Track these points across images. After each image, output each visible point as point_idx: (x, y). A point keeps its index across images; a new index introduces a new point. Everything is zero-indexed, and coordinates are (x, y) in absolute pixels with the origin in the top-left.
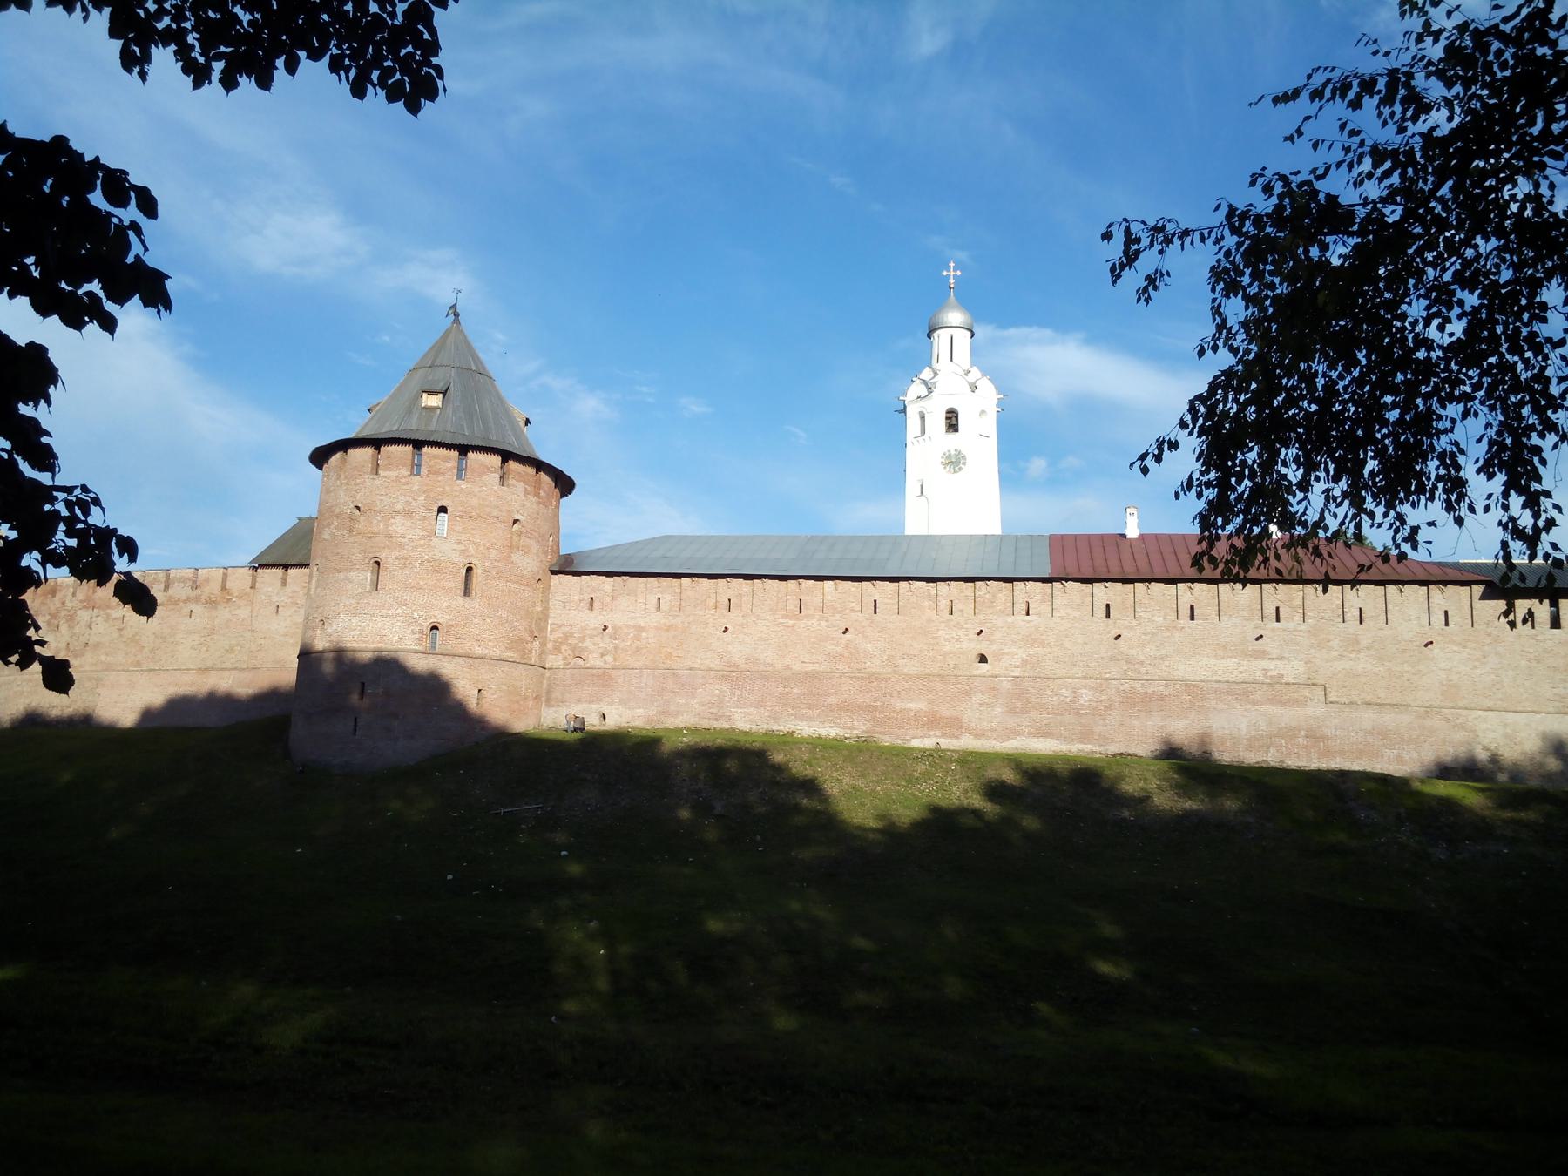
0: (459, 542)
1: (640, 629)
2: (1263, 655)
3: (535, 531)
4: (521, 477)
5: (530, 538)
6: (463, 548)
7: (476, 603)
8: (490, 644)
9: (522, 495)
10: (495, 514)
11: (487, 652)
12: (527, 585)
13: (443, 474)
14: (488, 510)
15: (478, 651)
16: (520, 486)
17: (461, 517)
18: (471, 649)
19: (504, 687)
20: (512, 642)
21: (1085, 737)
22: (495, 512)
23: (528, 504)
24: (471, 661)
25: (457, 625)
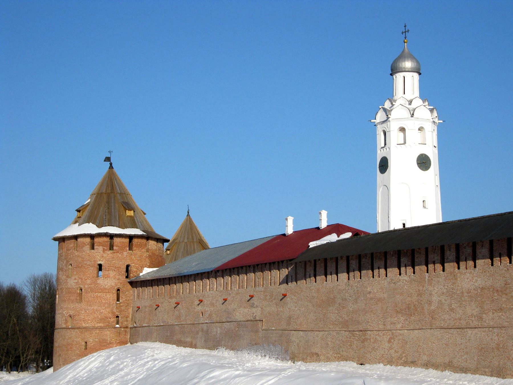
0: (75, 279)
1: (146, 307)
2: (252, 306)
3: (111, 266)
4: (100, 244)
5: (108, 271)
6: (77, 281)
8: (89, 322)
9: (102, 252)
11: (88, 325)
12: (108, 292)
13: (70, 250)
14: (85, 262)
15: (84, 325)
16: (101, 248)
17: (76, 268)
18: (81, 325)
19: (97, 340)
20: (100, 319)
22: (88, 263)
25: (76, 315)
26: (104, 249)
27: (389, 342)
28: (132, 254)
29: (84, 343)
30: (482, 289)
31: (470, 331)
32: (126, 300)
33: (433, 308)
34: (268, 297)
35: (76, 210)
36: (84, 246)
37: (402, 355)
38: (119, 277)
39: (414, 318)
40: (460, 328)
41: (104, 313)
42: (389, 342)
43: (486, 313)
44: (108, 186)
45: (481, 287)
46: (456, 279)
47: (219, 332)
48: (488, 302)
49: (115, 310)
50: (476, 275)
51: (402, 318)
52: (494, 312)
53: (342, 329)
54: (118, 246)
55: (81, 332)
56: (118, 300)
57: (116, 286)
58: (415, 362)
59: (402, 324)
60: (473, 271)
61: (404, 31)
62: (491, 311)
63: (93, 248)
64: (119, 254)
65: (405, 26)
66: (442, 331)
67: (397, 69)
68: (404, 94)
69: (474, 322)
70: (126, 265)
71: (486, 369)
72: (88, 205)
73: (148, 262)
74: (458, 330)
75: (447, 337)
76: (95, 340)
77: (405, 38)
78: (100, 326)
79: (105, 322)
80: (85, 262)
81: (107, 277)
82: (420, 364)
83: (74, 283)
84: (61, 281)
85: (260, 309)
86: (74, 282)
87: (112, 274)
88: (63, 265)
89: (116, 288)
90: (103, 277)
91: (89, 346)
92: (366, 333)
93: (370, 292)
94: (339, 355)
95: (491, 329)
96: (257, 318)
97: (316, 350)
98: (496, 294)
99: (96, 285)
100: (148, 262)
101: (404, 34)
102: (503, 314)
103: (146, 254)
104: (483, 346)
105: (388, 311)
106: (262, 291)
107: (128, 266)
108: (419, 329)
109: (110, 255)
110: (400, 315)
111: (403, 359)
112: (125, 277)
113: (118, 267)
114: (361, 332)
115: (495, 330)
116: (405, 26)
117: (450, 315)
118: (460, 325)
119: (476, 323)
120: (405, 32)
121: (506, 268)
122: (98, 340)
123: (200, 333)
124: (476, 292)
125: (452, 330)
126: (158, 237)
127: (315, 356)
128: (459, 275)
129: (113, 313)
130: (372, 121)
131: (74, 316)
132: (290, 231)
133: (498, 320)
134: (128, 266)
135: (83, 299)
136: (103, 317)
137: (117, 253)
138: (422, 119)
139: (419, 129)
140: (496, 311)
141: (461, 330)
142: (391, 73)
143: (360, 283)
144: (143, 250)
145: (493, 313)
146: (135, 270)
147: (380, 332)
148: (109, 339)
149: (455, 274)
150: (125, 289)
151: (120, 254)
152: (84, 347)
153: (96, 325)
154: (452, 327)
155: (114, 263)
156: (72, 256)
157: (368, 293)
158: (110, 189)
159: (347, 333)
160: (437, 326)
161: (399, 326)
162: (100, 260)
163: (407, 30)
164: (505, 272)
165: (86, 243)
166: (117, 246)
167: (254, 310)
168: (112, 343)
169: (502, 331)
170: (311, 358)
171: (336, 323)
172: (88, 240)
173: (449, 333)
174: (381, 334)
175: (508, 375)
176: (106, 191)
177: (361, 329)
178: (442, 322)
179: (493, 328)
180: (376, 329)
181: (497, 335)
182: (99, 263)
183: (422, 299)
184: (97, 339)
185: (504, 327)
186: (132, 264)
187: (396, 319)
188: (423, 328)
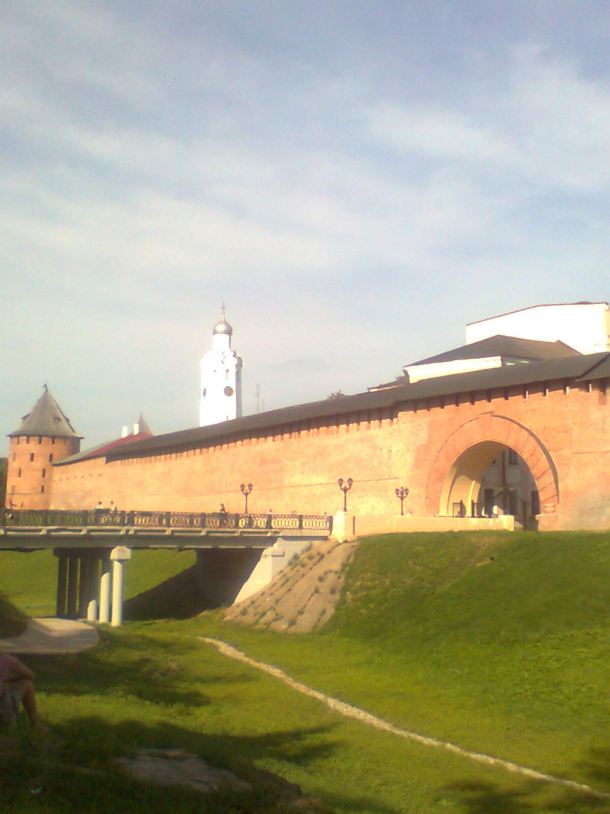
172: (25, 438)
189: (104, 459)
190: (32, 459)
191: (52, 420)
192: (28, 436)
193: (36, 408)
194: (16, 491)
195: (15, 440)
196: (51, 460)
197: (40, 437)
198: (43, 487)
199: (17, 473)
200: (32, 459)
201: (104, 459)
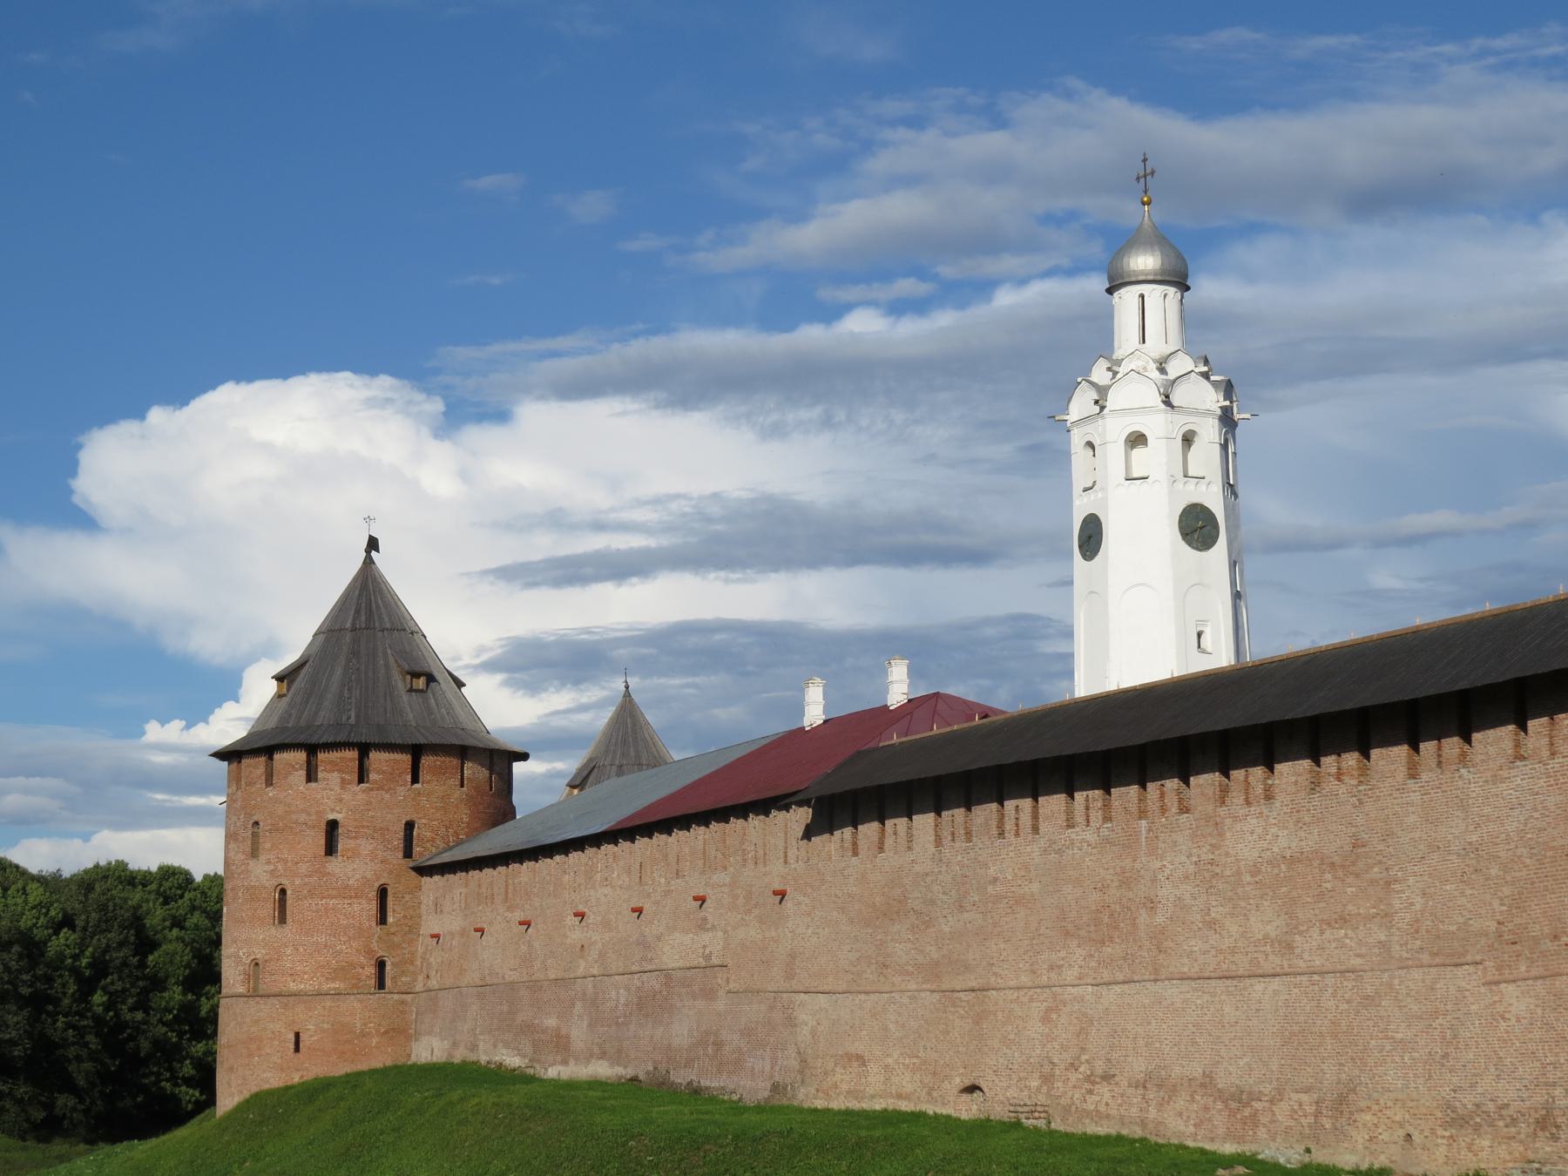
0: (268, 862)
1: (452, 934)
2: (702, 926)
3: (363, 827)
4: (334, 766)
5: (355, 838)
6: (272, 867)
7: (289, 931)
8: (306, 976)
9: (337, 788)
10: (303, 820)
11: (302, 987)
14: (294, 817)
15: (293, 986)
16: (335, 778)
18: (285, 986)
19: (325, 1026)
20: (335, 970)
21: (618, 1058)
22: (303, 818)
23: (346, 796)
24: (285, 1000)
26: (344, 783)
27: (1046, 1019)
28: (419, 793)
29: (291, 1037)
30: (1292, 861)
31: (1259, 986)
32: (405, 917)
33: (1160, 919)
34: (741, 901)
35: (272, 678)
36: (289, 773)
37: (1079, 1057)
38: (385, 854)
39: (1109, 950)
40: (1232, 978)
41: (347, 953)
42: (1046, 1019)
43: (1303, 931)
44: (358, 611)
45: (1288, 856)
46: (1221, 835)
47: (622, 1001)
48: (1309, 899)
49: (374, 946)
50: (1274, 821)
51: (1080, 951)
52: (1325, 927)
53: (924, 986)
54: (384, 772)
55: (285, 1006)
56: (382, 920)
57: (378, 879)
58: (1114, 1076)
59: (1081, 967)
60: (1265, 811)
61: (1142, 173)
62: (1317, 924)
63: (311, 777)
64: (384, 792)
65: (1145, 160)
66: (1185, 986)
67: (1123, 278)
68: (1144, 342)
69: (1271, 957)
70: (404, 822)
71: (1303, 1095)
72: (306, 662)
73: (466, 814)
74: (1228, 982)
75: (1199, 1002)
76: (321, 1025)
77: (1146, 192)
78: (335, 989)
79: (348, 976)
80: (294, 817)
81: (354, 854)
82: (1126, 1084)
83: (265, 874)
84: (234, 867)
85: (720, 934)
86: (264, 871)
87: (366, 846)
88: (238, 825)
89: (377, 885)
90: (343, 856)
91: (307, 1044)
92: (985, 997)
93: (996, 880)
94: (915, 1060)
95: (1316, 977)
96: (715, 961)
97: (858, 1047)
98: (1328, 876)
99: (323, 877)
100: (466, 814)
101: (1142, 180)
102: (1349, 932)
103: (459, 794)
104: (1296, 1028)
105: (1041, 932)
106: (725, 885)
107: (410, 826)
108: (1124, 982)
109: (361, 796)
110: (1075, 942)
111: (1082, 1069)
112: (401, 855)
113: (381, 829)
114: (973, 994)
115: (1330, 980)
116: (1145, 160)
117: (1205, 939)
118: (1234, 968)
119: (1274, 962)
120: (1145, 176)
121: (1354, 799)
122: (329, 1026)
123: (579, 1005)
124: (1276, 871)
125: (1213, 982)
126: (492, 746)
127: (855, 1064)
128: (1228, 821)
129: (369, 952)
130: (1057, 418)
131: (267, 961)
132: (814, 714)
133: (1337, 951)
134: (410, 826)
135: (288, 917)
136: (344, 964)
137: (378, 789)
138: (1196, 412)
139: (1183, 436)
140: (1329, 924)
141: (1235, 982)
142: (1108, 286)
143: (969, 853)
144: (451, 782)
145: (1322, 932)
146: (428, 834)
147: (1022, 993)
148: (358, 1025)
149: (1218, 819)
150: (401, 888)
151: (387, 791)
152: (292, 1046)
153: (325, 987)
154: (1213, 975)
155: (372, 817)
156: (259, 799)
157: (990, 883)
158: (363, 618)
159: (937, 996)
160: (1171, 973)
161: (1070, 975)
162: (333, 810)
163: (1148, 171)
164: (1353, 810)
165: (297, 763)
166: (378, 773)
167: (706, 937)
168: (369, 1033)
169: (1345, 983)
170: (845, 1068)
171: (911, 969)
172: (300, 756)
173: (1204, 992)
174: (1026, 999)
175: (1362, 1111)
176: (354, 624)
177: (974, 984)
178: (1186, 961)
179: (1322, 973)
180: (1012, 983)
181: (1334, 995)
182: (331, 817)
183: (1130, 895)
184: (328, 1023)
185: (1353, 972)
186: (420, 818)
187: (1063, 954)
188: (1136, 978)
189: (801, 816)
190: (330, 849)
191: (400, 684)
192: (312, 749)
193: (330, 632)
194: (267, 983)
195: (254, 767)
196: (408, 853)
197: (364, 749)
198: (381, 965)
199: (268, 909)
200: (330, 849)
201: (801, 816)
